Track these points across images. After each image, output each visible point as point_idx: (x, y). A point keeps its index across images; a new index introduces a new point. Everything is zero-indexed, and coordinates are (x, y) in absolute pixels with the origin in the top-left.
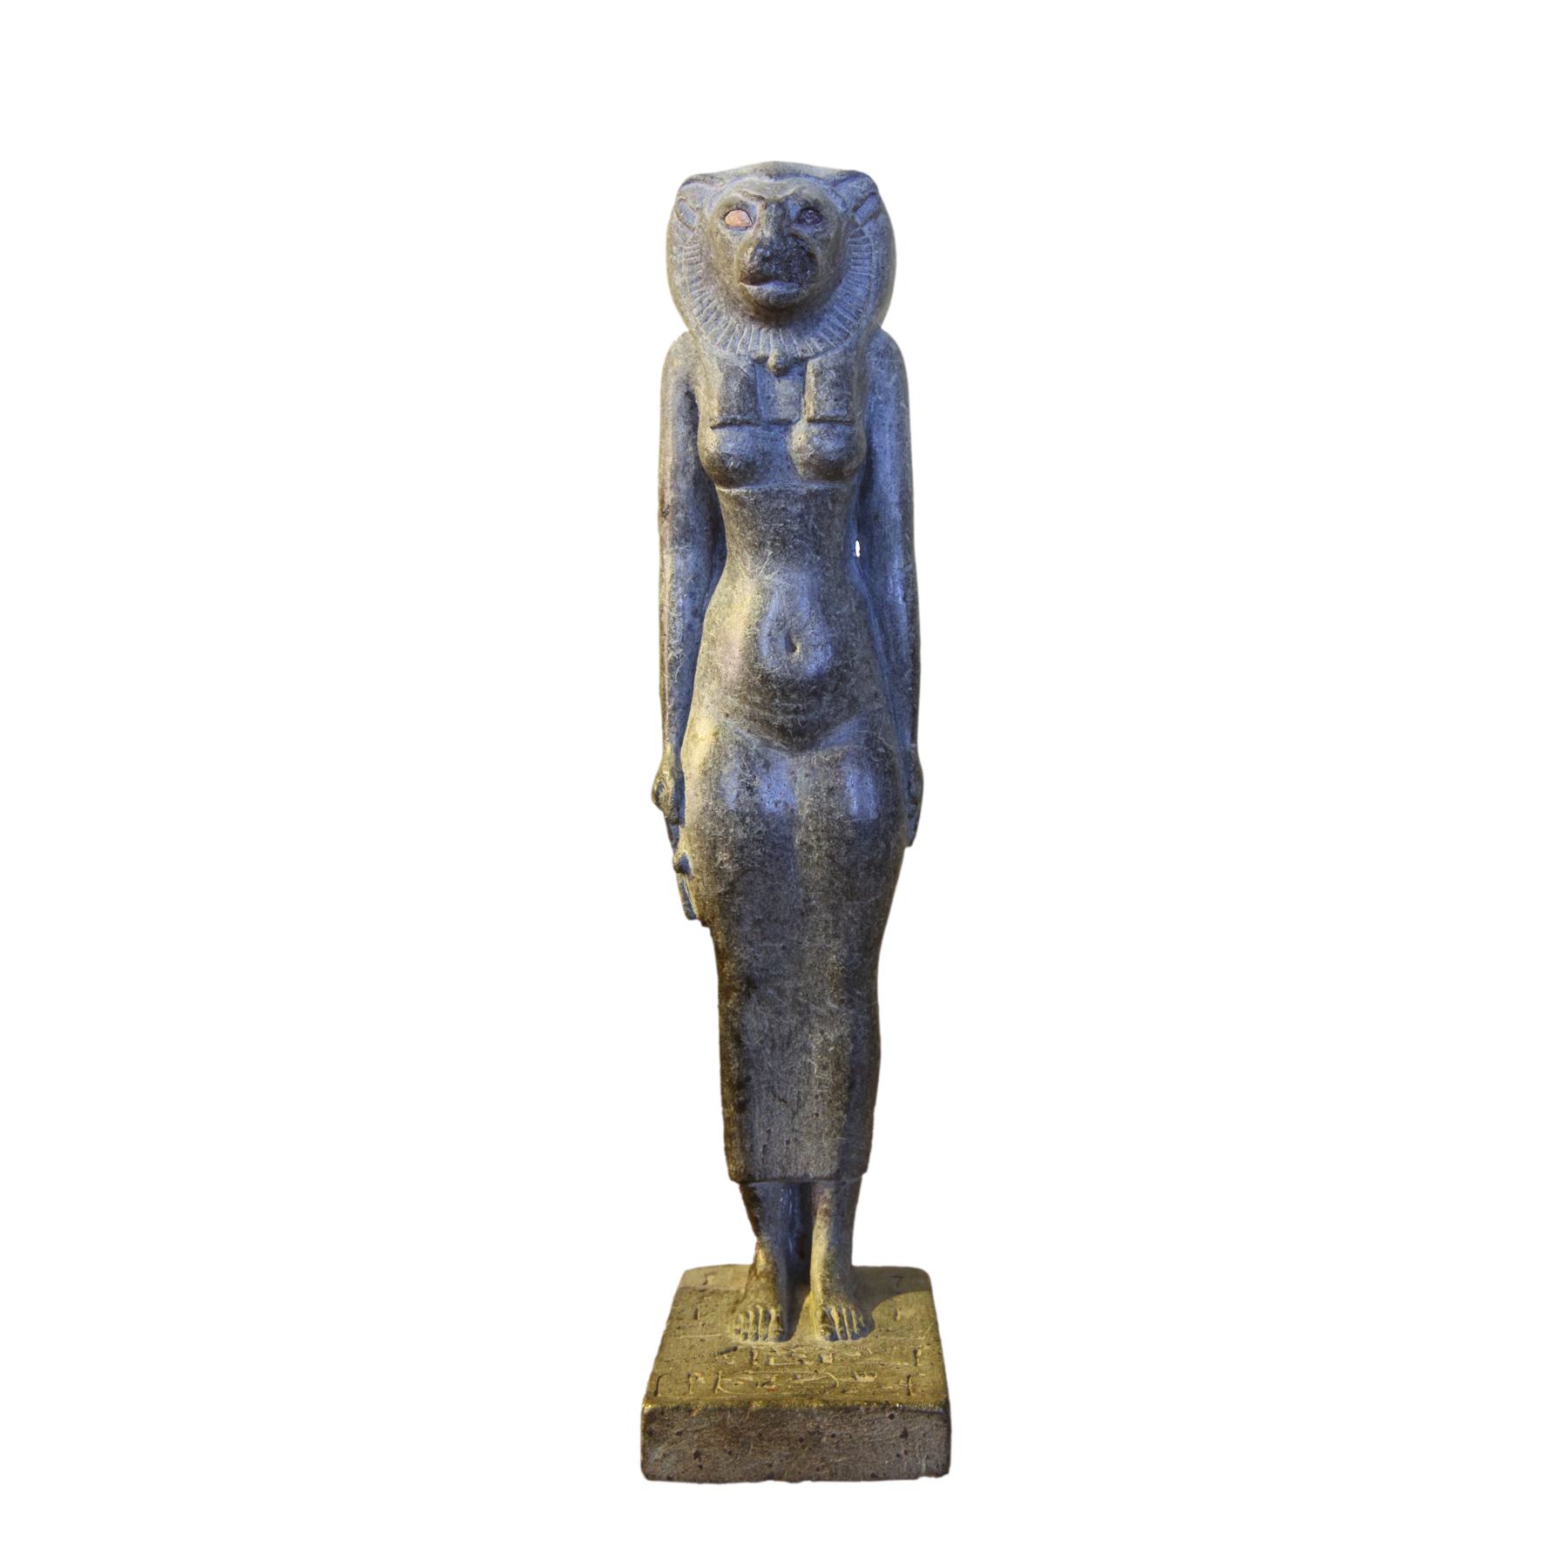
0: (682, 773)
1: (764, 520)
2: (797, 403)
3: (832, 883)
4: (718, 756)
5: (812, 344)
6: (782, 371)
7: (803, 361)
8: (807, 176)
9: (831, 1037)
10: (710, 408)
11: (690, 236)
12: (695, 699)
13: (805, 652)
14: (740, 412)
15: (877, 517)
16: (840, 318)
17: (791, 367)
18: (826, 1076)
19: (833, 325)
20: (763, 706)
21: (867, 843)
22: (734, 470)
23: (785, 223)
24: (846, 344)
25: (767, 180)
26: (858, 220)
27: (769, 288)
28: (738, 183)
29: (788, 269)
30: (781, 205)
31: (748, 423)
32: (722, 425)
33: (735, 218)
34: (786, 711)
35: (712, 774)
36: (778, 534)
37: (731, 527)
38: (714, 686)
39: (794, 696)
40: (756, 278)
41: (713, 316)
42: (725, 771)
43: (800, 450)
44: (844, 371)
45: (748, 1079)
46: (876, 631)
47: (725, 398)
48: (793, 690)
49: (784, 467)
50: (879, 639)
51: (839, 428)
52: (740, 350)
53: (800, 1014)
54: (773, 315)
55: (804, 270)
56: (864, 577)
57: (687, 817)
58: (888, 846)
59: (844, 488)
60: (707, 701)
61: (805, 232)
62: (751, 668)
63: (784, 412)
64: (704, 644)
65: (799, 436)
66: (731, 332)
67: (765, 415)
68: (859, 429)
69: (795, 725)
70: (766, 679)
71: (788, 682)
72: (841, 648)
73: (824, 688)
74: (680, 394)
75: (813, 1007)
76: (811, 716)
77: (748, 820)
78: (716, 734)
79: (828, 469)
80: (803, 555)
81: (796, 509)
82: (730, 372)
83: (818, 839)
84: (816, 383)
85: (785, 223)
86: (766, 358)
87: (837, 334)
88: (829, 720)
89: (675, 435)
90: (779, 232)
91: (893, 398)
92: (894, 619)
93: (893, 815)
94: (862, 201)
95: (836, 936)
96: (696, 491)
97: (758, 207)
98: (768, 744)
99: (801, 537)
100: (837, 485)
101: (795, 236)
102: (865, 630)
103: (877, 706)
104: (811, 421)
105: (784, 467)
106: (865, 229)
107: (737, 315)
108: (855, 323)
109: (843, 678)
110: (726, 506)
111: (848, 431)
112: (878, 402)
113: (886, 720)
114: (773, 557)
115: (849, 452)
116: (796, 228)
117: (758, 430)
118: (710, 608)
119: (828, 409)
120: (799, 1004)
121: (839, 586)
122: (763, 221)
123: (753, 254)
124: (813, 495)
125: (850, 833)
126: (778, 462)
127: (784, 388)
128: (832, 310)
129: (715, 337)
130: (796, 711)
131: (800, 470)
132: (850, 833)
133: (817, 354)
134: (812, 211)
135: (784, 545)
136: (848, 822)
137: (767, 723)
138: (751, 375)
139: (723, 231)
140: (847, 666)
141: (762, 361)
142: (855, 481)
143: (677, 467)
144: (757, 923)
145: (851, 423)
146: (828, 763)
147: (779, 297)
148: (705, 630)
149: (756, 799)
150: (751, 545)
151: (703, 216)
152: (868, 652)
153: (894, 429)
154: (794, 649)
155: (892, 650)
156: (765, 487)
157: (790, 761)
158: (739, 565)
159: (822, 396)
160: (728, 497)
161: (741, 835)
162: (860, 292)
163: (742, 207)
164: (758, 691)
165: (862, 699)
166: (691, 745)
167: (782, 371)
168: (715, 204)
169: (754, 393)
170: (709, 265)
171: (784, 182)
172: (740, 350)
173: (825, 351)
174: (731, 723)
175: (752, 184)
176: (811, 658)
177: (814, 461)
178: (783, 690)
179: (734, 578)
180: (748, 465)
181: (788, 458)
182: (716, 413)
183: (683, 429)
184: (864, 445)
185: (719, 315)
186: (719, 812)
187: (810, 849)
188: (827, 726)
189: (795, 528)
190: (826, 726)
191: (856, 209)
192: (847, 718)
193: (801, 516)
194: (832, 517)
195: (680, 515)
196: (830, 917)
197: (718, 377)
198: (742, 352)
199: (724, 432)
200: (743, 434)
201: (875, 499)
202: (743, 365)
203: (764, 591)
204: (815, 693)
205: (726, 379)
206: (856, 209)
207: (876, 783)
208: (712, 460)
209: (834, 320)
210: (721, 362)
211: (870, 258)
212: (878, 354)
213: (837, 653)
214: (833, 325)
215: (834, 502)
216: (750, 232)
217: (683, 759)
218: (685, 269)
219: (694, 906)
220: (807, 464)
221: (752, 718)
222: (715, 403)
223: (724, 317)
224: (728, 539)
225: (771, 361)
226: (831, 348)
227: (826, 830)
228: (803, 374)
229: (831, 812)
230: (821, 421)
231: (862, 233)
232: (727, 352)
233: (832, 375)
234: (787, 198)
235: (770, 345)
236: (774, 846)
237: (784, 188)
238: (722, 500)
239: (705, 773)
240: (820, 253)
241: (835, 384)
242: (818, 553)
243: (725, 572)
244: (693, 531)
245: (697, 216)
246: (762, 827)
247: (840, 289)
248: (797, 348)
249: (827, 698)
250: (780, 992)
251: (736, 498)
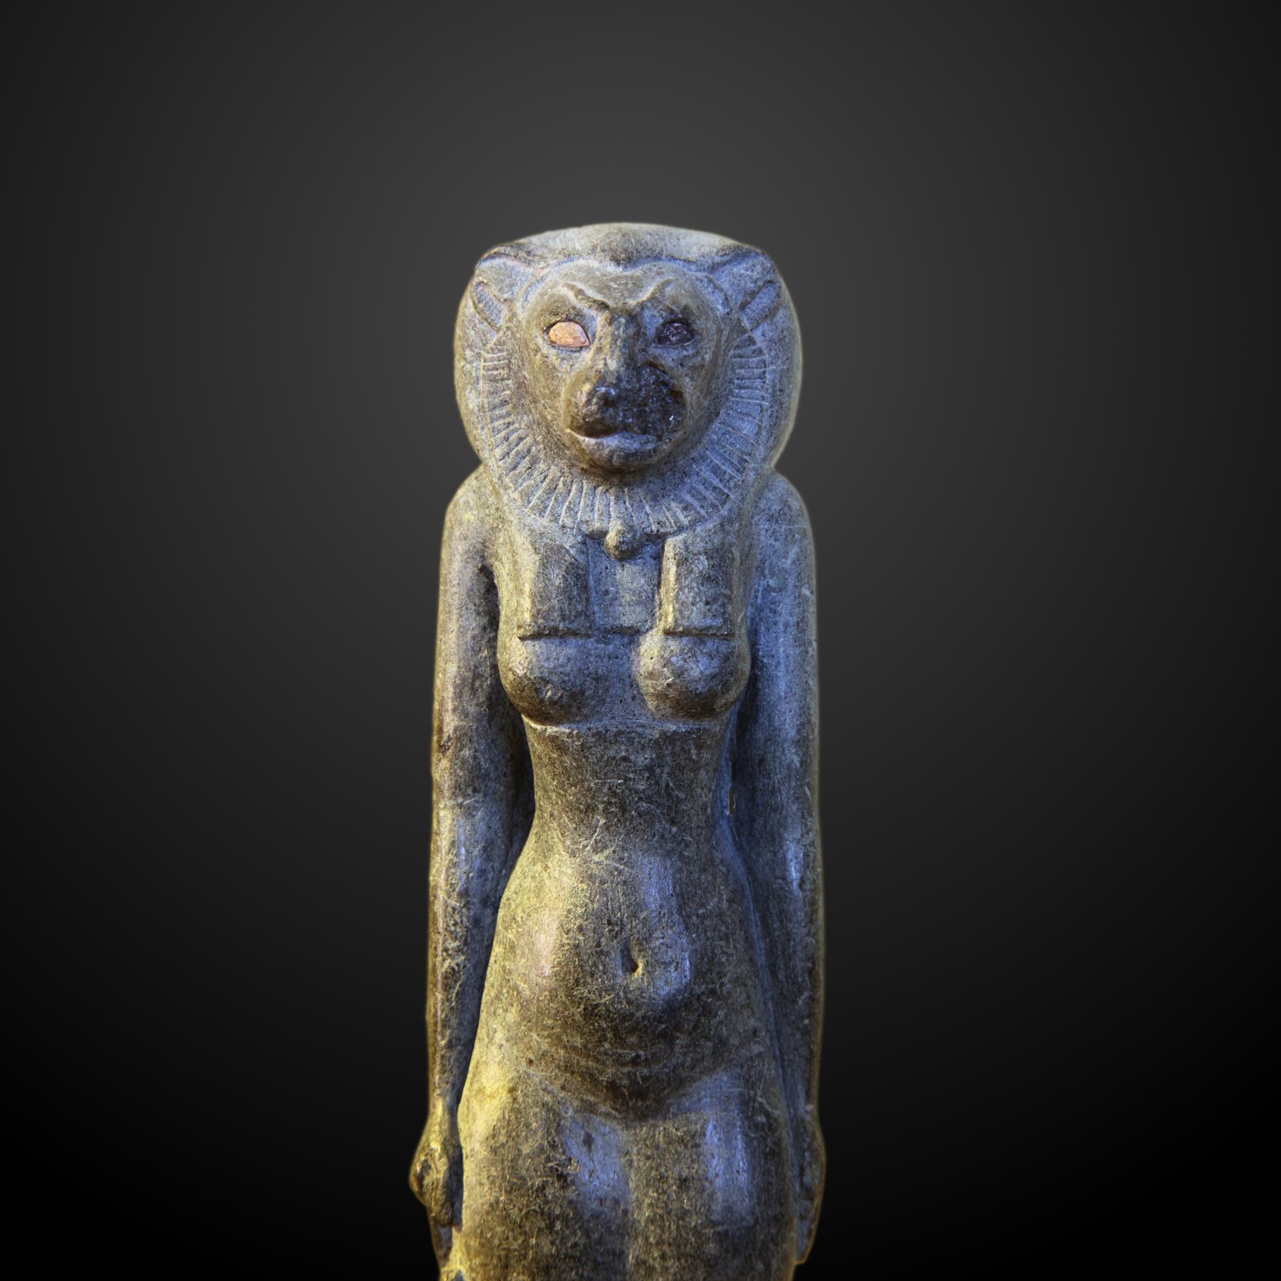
0: (459, 1148)
1: (595, 774)
2: (649, 602)
4: (514, 1120)
5: (672, 513)
6: (628, 553)
7: (658, 539)
8: (672, 258)
10: (518, 604)
11: (493, 339)
12: (482, 1032)
13: (649, 971)
14: (563, 618)
15: (762, 761)
16: (715, 470)
17: (643, 548)
19: (705, 483)
20: (585, 1051)
21: (736, 1263)
22: (553, 703)
23: (640, 344)
24: (724, 512)
25: (612, 269)
26: (746, 323)
27: (612, 442)
28: (568, 267)
29: (641, 415)
30: (633, 317)
31: (575, 634)
32: (536, 636)
33: (564, 332)
34: (619, 1061)
35: (502, 1146)
36: (615, 794)
37: (542, 776)
38: (512, 1016)
39: (633, 1039)
40: (592, 429)
41: (525, 463)
42: (526, 1150)
43: (651, 675)
44: (720, 556)
46: (756, 932)
47: (540, 597)
48: (632, 1031)
49: (628, 696)
50: (761, 945)
51: (710, 645)
52: (564, 519)
54: (615, 474)
55: (666, 414)
56: (739, 848)
57: (466, 1216)
58: (768, 1267)
59: (713, 726)
60: (500, 1037)
61: (668, 357)
62: (569, 995)
63: (629, 618)
64: (497, 950)
65: (651, 653)
66: (552, 490)
67: (600, 619)
68: (741, 644)
69: (633, 1082)
70: (591, 1012)
71: (624, 1018)
72: (705, 966)
73: (677, 1028)
74: (471, 570)
76: (656, 1068)
77: (558, 1226)
78: (512, 1090)
79: (692, 703)
80: (651, 825)
81: (643, 759)
82: (549, 555)
83: (663, 1257)
84: (678, 575)
85: (640, 344)
86: (604, 534)
87: (710, 496)
88: (684, 1073)
89: (462, 631)
90: (630, 362)
91: (791, 581)
92: (783, 916)
93: (776, 1219)
94: (753, 294)
96: (491, 718)
97: (600, 321)
98: (588, 1109)
99: (649, 800)
100: (705, 724)
101: (653, 365)
102: (739, 934)
103: (756, 1049)
104: (668, 633)
105: (628, 696)
106: (757, 335)
107: (562, 463)
108: (738, 477)
109: (707, 1012)
110: (536, 748)
111: (723, 648)
112: (768, 589)
113: (769, 1069)
114: (607, 827)
115: (722, 678)
116: (655, 351)
117: (591, 644)
118: (506, 894)
119: (696, 617)
121: (704, 870)
122: (606, 343)
123: (591, 394)
124: (669, 738)
125: (711, 1248)
126: (617, 690)
127: (628, 578)
128: (703, 458)
129: (526, 496)
130: (635, 1062)
131: (651, 704)
132: (711, 1248)
133: (681, 529)
134: (681, 325)
135: (624, 810)
136: (709, 1232)
137: (590, 1077)
138: (581, 559)
139: (545, 349)
140: (713, 993)
141: (597, 537)
142: (730, 716)
143: (464, 680)
145: (730, 635)
146: (681, 1141)
147: (628, 456)
148: (499, 927)
149: (571, 1194)
150: (570, 807)
151: (514, 315)
152: (745, 969)
153: (793, 630)
154: (634, 968)
155: (781, 963)
156: (596, 725)
157: (623, 1136)
158: (555, 834)
159: (688, 596)
160: (541, 736)
161: (547, 1248)
162: (747, 428)
163: (575, 317)
164: (578, 1028)
165: (734, 1041)
166: (475, 1104)
167: (628, 553)
168: (533, 298)
169: (585, 588)
170: (520, 385)
171: (637, 272)
172: (564, 519)
173: (692, 525)
174: (537, 1074)
175: (589, 271)
176: (656, 978)
177: (672, 693)
178: (615, 1030)
179: (546, 852)
180: (573, 696)
181: (633, 684)
182: (527, 617)
183: (474, 624)
184: (746, 667)
185: (534, 461)
186: (514, 1213)
188: (681, 1082)
189: (641, 786)
190: (678, 1082)
191: (743, 307)
192: (711, 1070)
193: (650, 769)
194: (696, 770)
195: (466, 753)
197: (529, 562)
198: (568, 522)
199: (538, 646)
200: (570, 650)
201: (760, 735)
202: (569, 542)
203: (591, 877)
204: (663, 1035)
205: (544, 565)
206: (743, 307)
207: (752, 1169)
208: (520, 682)
209: (706, 474)
210: (536, 539)
211: (762, 376)
212: (771, 519)
213: (698, 973)
214: (705, 483)
215: (699, 747)
216: (587, 356)
217: (461, 1125)
218: (483, 386)
220: (662, 696)
221: (568, 1068)
222: (527, 603)
223: (542, 466)
224: (538, 794)
225: (611, 539)
226: (699, 520)
227: (676, 1243)
228: (659, 557)
229: (684, 1214)
230: (686, 633)
231: (752, 341)
232: (545, 521)
233: (702, 564)
234: (642, 306)
235: (609, 515)
236: (597, 1265)
237: (638, 285)
238: (531, 737)
239: (494, 1150)
240: (689, 388)
241: (706, 579)
242: (673, 823)
243: (532, 839)
244: (487, 775)
245: (505, 312)
246: (579, 1238)
247: (716, 425)
248: (650, 519)
249: (682, 1040)
251: (553, 739)
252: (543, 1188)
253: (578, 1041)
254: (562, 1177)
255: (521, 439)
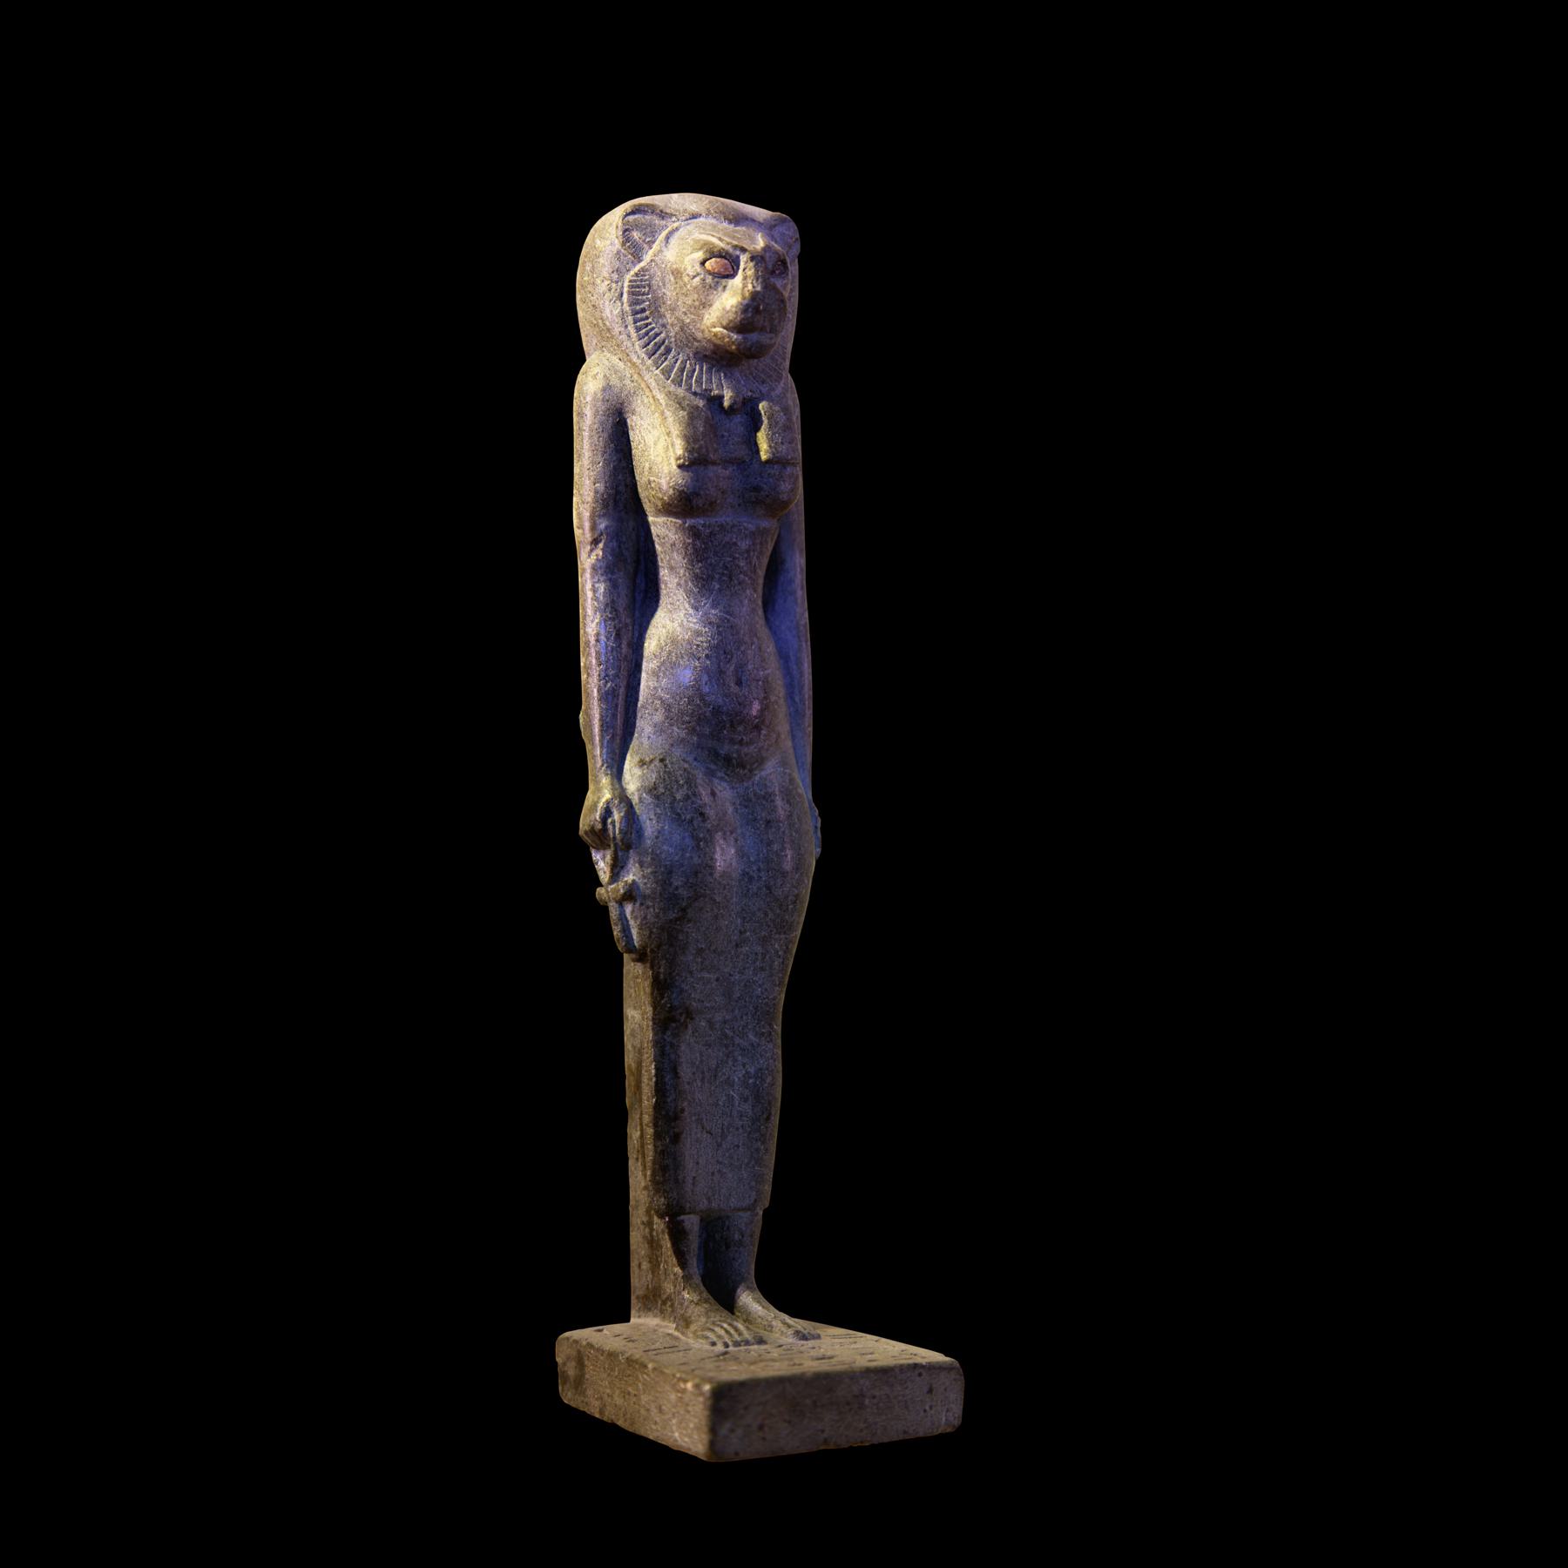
1: (716, 554)
3: (766, 914)
9: (752, 1070)
18: (747, 1107)
38: (659, 717)
39: (740, 728)
42: (678, 797)
45: (683, 1111)
53: (726, 1046)
60: (648, 730)
75: (737, 1040)
81: (744, 545)
95: (762, 969)
114: (720, 590)
120: (726, 1036)
129: (667, 373)
144: (700, 951)
185: (668, 351)
187: (751, 879)
193: (748, 551)
196: (759, 949)
219: (634, 932)
225: (726, 404)
239: (657, 797)
250: (711, 1024)
252: (691, 821)
253: (707, 731)
254: (702, 814)
255: (657, 335)
